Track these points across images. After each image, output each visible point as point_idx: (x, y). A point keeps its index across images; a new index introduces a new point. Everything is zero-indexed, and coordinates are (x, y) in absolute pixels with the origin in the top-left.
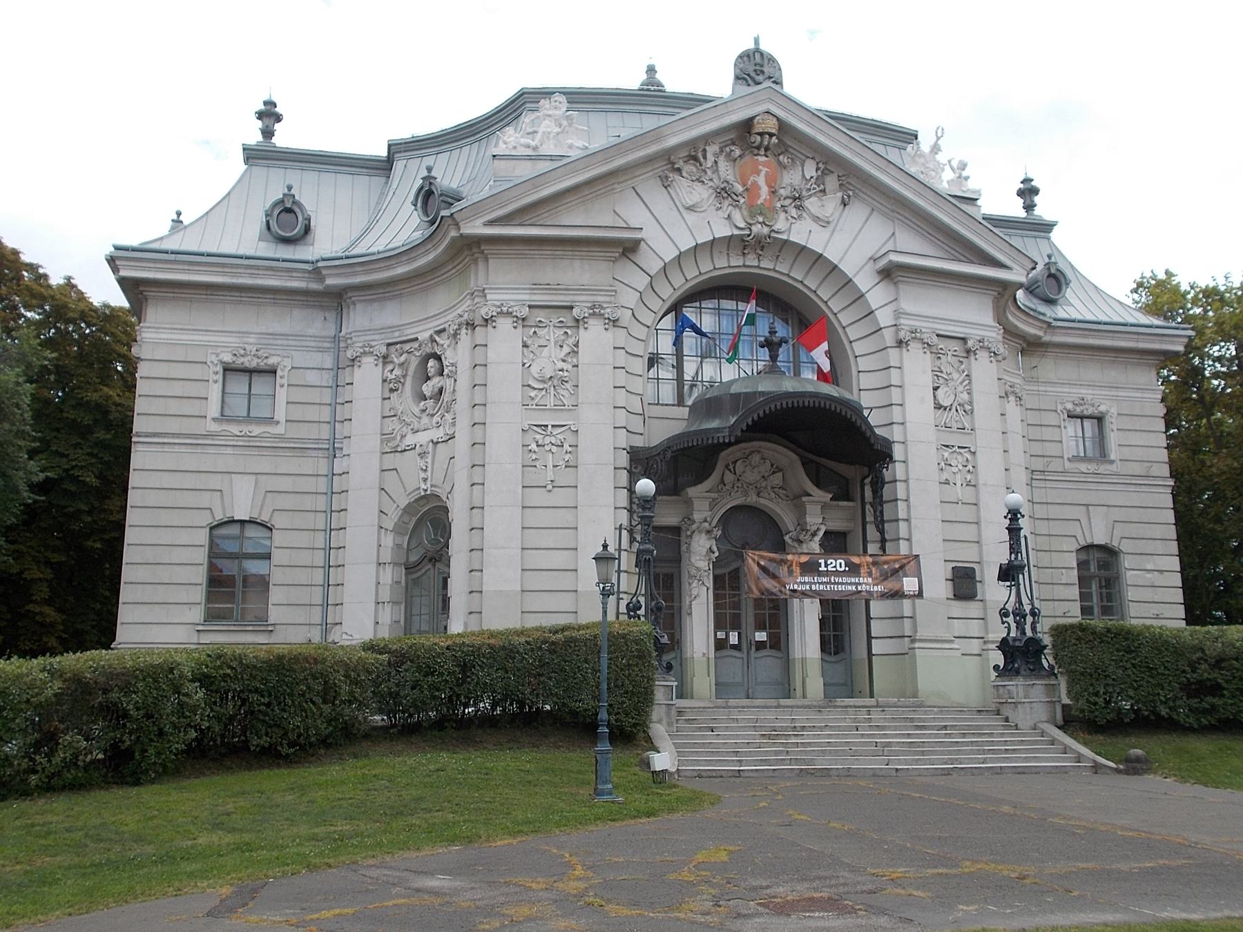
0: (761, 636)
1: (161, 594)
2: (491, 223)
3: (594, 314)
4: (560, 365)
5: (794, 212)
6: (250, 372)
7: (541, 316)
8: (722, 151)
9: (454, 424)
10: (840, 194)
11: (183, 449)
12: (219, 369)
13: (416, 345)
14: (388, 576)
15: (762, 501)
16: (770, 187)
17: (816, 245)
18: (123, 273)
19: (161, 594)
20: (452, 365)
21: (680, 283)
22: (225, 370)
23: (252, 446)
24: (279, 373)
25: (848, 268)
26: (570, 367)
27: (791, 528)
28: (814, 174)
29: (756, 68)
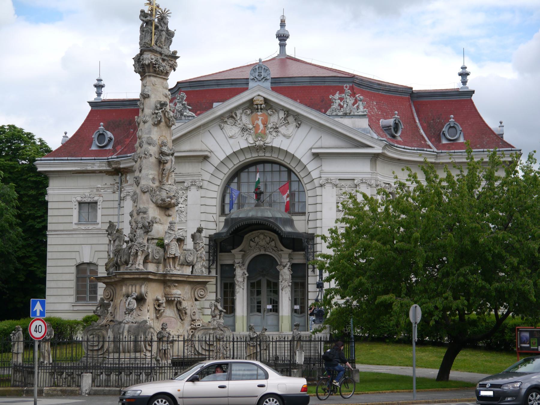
0: (270, 307)
1: (59, 292)
3: (192, 185)
5: (274, 134)
10: (295, 124)
11: (65, 236)
12: (77, 203)
15: (267, 253)
16: (264, 124)
19: (59, 292)
23: (88, 233)
24: (98, 203)
25: (298, 155)
26: (184, 206)
28: (283, 116)
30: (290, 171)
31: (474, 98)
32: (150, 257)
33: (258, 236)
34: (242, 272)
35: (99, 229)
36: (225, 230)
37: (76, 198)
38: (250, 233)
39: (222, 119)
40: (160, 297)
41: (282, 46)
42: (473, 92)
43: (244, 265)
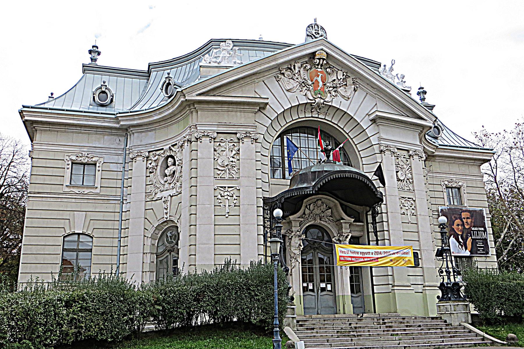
2: (200, 95)
3: (246, 136)
4: (231, 159)
5: (334, 93)
6: (84, 164)
7: (222, 136)
8: (302, 65)
9: (181, 187)
11: (52, 200)
12: (70, 163)
13: (162, 151)
14: (148, 259)
15: (322, 222)
16: (323, 82)
18: (26, 118)
20: (180, 160)
21: (284, 124)
22: (72, 163)
24: (98, 165)
26: (236, 160)
27: (336, 235)
28: (342, 77)
29: (315, 31)
35: (97, 194)
37: (69, 156)
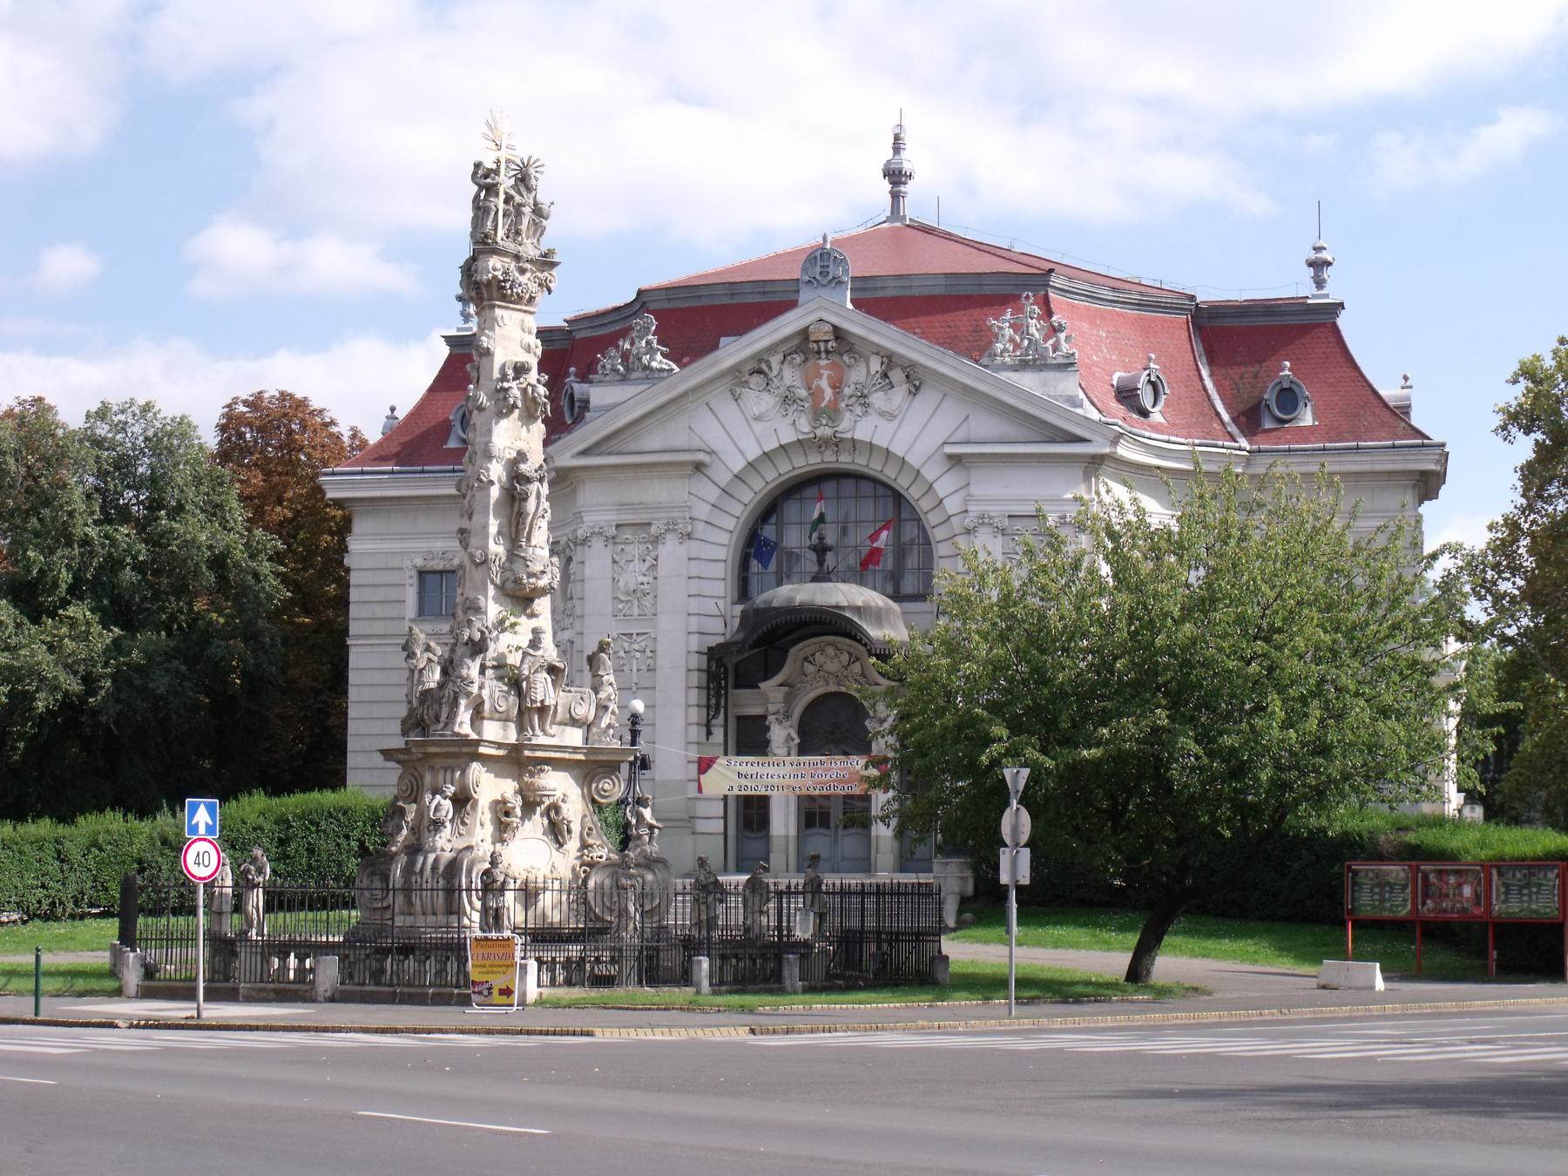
2: (584, 453)
3: (668, 530)
4: (641, 579)
5: (858, 410)
6: (441, 572)
7: (627, 534)
10: (905, 387)
11: (388, 649)
12: (414, 573)
16: (834, 387)
17: (881, 441)
25: (914, 460)
30: (898, 498)
31: (1343, 321)
32: (487, 706)
33: (822, 651)
34: (784, 734)
36: (740, 636)
38: (801, 645)
39: (737, 378)
40: (509, 795)
41: (896, 196)
42: (1341, 305)
43: (787, 717)
